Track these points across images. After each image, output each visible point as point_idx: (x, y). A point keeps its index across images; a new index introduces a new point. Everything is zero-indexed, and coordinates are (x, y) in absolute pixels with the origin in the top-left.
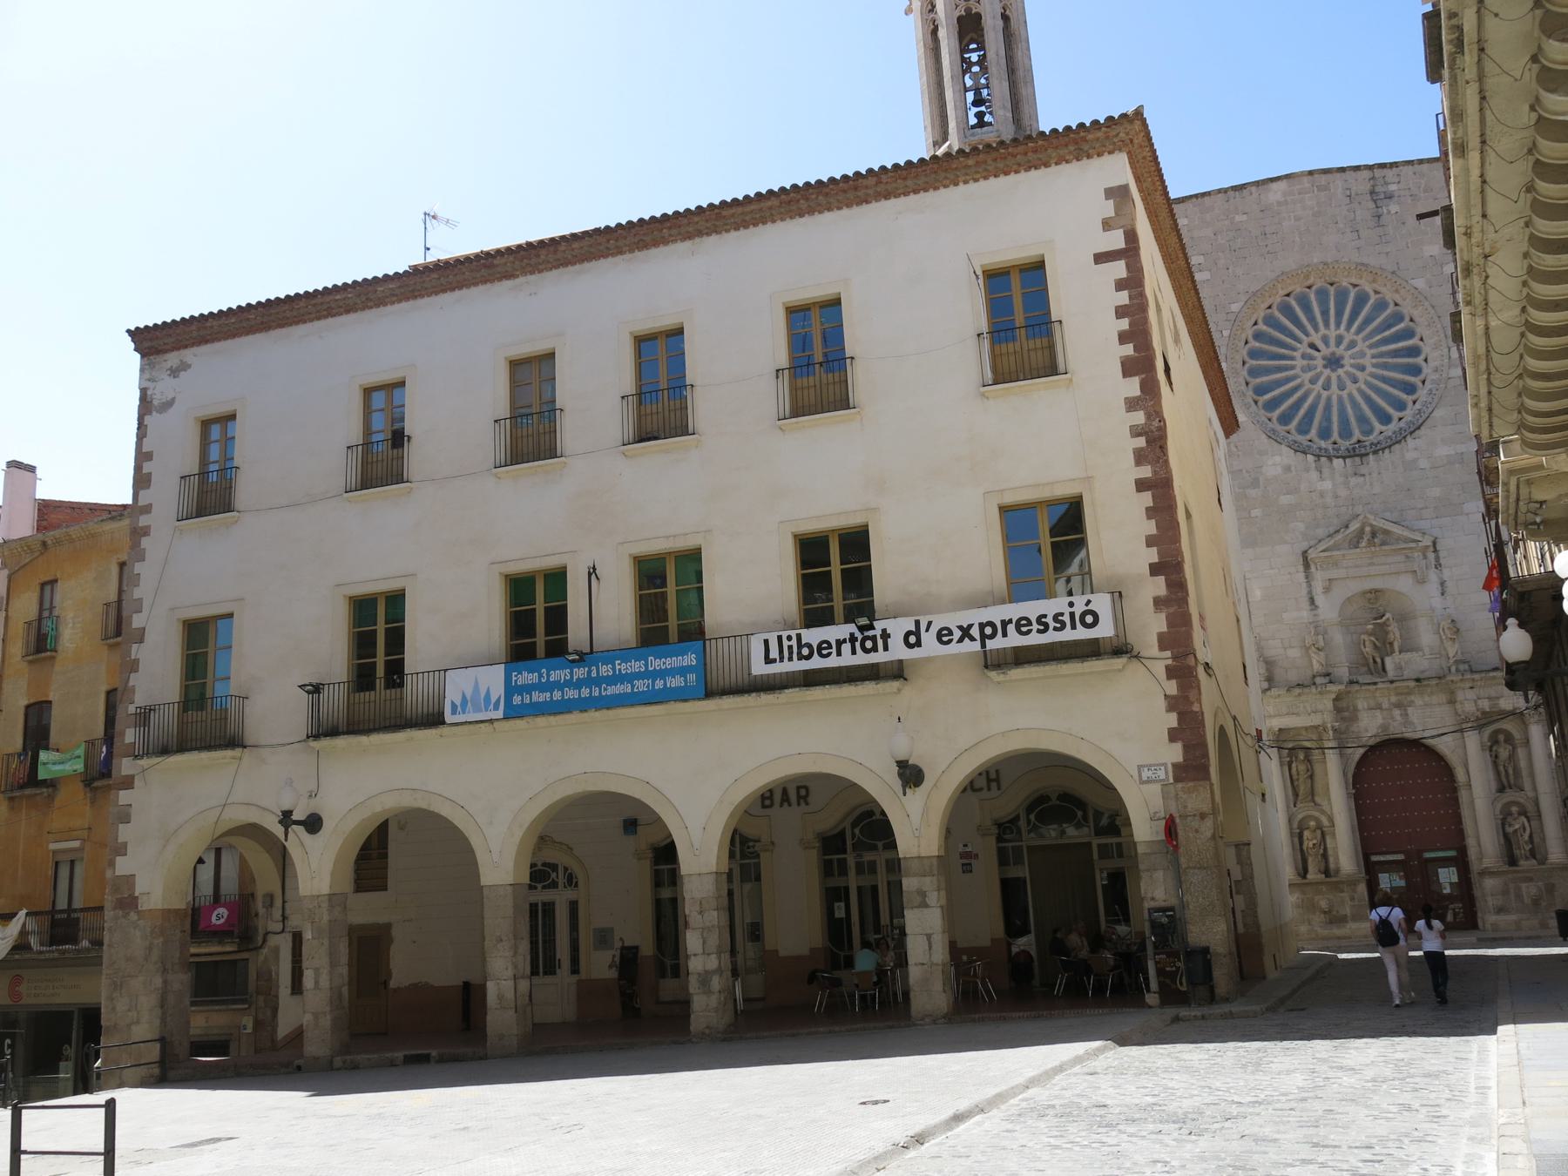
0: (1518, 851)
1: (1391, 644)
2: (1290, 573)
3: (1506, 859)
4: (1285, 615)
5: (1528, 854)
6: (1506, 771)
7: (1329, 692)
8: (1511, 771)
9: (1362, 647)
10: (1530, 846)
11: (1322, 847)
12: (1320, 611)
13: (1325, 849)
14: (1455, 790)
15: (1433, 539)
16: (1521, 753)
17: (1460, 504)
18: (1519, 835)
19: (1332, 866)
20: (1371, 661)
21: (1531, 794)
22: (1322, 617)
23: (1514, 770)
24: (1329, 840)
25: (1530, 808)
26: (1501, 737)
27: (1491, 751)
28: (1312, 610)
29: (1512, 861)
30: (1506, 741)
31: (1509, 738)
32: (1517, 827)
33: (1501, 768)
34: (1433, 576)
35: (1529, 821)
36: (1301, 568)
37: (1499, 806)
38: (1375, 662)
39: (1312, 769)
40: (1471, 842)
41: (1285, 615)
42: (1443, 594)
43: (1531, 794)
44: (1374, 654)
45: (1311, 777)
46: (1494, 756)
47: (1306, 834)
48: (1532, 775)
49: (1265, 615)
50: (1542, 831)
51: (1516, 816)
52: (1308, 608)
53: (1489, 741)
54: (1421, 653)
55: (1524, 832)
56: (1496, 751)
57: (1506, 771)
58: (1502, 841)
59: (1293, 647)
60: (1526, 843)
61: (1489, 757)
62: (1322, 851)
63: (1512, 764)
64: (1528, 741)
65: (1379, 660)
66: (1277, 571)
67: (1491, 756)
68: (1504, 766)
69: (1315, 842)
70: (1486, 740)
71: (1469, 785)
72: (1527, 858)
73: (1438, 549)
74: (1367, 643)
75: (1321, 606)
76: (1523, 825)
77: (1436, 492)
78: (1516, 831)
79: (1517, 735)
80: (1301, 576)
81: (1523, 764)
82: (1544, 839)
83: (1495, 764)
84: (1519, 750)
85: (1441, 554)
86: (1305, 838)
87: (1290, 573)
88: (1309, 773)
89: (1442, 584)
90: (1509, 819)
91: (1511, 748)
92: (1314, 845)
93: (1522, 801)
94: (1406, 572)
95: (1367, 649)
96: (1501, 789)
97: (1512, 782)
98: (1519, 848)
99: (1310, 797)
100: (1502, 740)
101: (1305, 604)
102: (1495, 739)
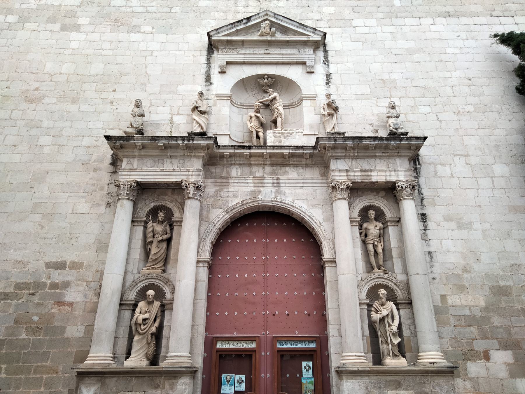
0: (385, 346)
1: (275, 122)
2: (193, 55)
3: (371, 355)
4: (179, 87)
5: (397, 352)
6: (375, 251)
7: (198, 147)
8: (380, 250)
9: (248, 123)
11: (157, 324)
12: (213, 87)
13: (160, 328)
14: (322, 269)
15: (322, 34)
16: (392, 231)
17: (350, 20)
18: (387, 325)
19: (163, 350)
20: (255, 135)
21: (401, 277)
22: (214, 92)
23: (384, 250)
24: (167, 313)
25: (400, 294)
26: (372, 214)
27: (360, 229)
28: (206, 86)
29: (378, 359)
30: (376, 219)
31: (380, 216)
32: (384, 312)
33: (371, 247)
34: (320, 69)
35: (398, 309)
36: (205, 53)
37: (366, 289)
38: (258, 137)
39: (172, 233)
40: (332, 330)
41: (179, 87)
42: (327, 84)
43: (401, 277)
44: (258, 130)
45: (169, 241)
46: (363, 234)
47: (142, 304)
48: (403, 256)
49: (162, 85)
50: (414, 323)
51: (384, 300)
52: (204, 83)
53: (359, 215)
54: (300, 130)
55: (393, 322)
56: (366, 229)
57: (375, 251)
58: (367, 333)
59: (181, 114)
60: (394, 334)
61: (358, 234)
62: (154, 329)
63: (382, 243)
64: (400, 218)
65: (261, 134)
66: (182, 53)
67: (361, 234)
68: (373, 244)
69: (147, 316)
70: (357, 216)
71: (334, 262)
72: (395, 356)
73: (327, 49)
74: (253, 119)
75: (215, 84)
76: (392, 312)
77: (332, 10)
78: (382, 320)
79: (389, 214)
80: (203, 59)
81: (394, 244)
82: (415, 333)
83: (364, 242)
84: (390, 228)
85: (330, 53)
86: (138, 310)
87: (193, 55)
88: (165, 237)
89: (328, 76)
90: (376, 304)
91: (381, 225)
92: (144, 320)
93: (391, 284)
94: (297, 63)
95: (252, 124)
96: (370, 268)
97: (381, 262)
98: (387, 342)
99: (161, 264)
100: (373, 216)
101: (202, 79)
102: (364, 213)
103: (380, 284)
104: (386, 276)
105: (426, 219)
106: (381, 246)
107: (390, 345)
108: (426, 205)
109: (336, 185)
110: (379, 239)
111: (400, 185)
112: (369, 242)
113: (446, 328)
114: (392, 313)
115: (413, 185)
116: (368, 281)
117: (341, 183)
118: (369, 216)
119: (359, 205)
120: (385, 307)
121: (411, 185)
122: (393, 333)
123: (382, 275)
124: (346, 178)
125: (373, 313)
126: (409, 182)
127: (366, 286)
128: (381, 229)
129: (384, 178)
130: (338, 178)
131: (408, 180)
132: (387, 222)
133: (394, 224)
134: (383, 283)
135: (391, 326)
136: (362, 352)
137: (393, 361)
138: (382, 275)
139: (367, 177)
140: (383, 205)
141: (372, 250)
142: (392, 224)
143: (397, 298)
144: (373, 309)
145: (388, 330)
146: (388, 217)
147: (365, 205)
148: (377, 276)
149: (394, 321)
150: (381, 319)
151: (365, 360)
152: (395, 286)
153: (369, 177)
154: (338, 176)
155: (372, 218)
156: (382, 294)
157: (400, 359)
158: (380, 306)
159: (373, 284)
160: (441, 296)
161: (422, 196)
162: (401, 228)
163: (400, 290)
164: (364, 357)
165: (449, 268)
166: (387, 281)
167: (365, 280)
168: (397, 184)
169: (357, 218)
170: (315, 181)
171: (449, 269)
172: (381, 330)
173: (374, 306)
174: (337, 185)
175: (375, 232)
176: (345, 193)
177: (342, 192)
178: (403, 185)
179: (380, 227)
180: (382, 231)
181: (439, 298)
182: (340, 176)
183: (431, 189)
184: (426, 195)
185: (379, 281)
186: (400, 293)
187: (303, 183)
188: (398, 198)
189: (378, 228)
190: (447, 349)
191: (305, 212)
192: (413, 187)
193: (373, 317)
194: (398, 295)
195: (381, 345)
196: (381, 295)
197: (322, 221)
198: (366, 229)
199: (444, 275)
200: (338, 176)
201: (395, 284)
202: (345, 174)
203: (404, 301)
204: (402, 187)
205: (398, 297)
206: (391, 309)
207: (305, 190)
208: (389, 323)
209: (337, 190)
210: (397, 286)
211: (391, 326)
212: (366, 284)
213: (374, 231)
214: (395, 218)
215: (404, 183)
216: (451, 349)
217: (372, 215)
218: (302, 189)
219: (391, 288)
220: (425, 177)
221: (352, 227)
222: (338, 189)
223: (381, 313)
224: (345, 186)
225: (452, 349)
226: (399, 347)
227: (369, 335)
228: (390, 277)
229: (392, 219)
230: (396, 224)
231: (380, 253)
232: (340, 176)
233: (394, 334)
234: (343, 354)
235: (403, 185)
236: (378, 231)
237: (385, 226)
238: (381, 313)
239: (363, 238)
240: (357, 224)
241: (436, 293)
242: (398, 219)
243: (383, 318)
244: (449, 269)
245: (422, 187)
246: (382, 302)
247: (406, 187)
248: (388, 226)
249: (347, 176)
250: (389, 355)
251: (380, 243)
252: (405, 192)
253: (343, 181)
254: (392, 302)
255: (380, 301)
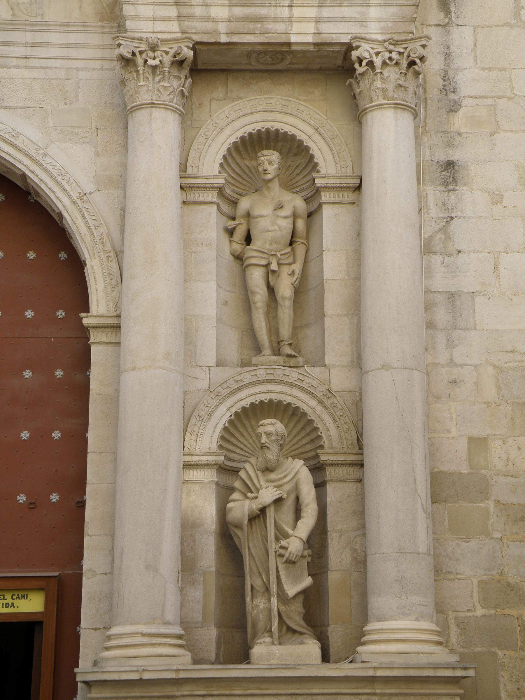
6: (271, 290)
10: (308, 581)
51: (272, 455)
56: (248, 215)
57: (271, 290)
63: (297, 267)
67: (231, 232)
76: (296, 488)
84: (327, 212)
97: (285, 332)
100: (272, 170)
103: (271, 401)
104: (293, 375)
105: (455, 181)
106: (293, 273)
107: (274, 601)
108: (463, 130)
109: (134, 54)
110: (289, 249)
111: (366, 55)
112: (253, 261)
113: (474, 544)
114: (297, 499)
115: (412, 55)
116: (228, 391)
117: (153, 48)
118: (261, 169)
119: (227, 131)
120: (273, 476)
121: (405, 55)
122: (288, 558)
123: (280, 372)
124: (174, 26)
125: (235, 496)
126: (397, 43)
127: (223, 408)
128: (299, 217)
129: (311, 28)
130: (148, 26)
131: (396, 37)
132: (318, 191)
133: (341, 199)
134: (281, 397)
135: (286, 536)
136: (168, 623)
137: (277, 649)
138: (279, 372)
139: (251, 26)
140: (310, 131)
141: (258, 290)
142: (337, 199)
143: (321, 447)
144: (237, 484)
145: (274, 550)
146: (323, 172)
147: (249, 129)
148: (262, 373)
149: (299, 523)
150: (258, 516)
151: (180, 646)
152: (319, 409)
153: (259, 25)
154: (147, 19)
155: (269, 177)
156: (268, 434)
157: (302, 643)
158: (259, 473)
159: (246, 403)
160: (471, 440)
161: (453, 97)
162: (361, 211)
163: (335, 421)
164: (180, 637)
165: (509, 348)
166: (296, 392)
167: (220, 389)
168: (354, 54)
169: (214, 177)
170: (73, 38)
171: (512, 352)
172: (253, 551)
173: (242, 474)
174: (141, 52)
175: (276, 228)
176: (166, 84)
177: (157, 79)
178: (377, 54)
179: (295, 209)
180: (301, 224)
181: (462, 446)
182: (154, 19)
183: (490, 69)
184: (468, 94)
185: (268, 392)
186: (333, 430)
187: (33, 45)
188: (363, 103)
189: (287, 211)
190: (469, 611)
191: (33, 152)
192: (412, 63)
193: (231, 509)
194: (325, 439)
195: (248, 600)
196: (264, 439)
197: (89, 187)
198: (248, 215)
199: (491, 370)
200: (147, 19)
201: (320, 402)
202: (173, 12)
203: (341, 458)
204: (371, 64)
205: (326, 445)
206: (292, 484)
207: (35, 73)
208: (277, 527)
209: (137, 72)
210: (325, 407)
211: (286, 536)
212: (221, 402)
213: (273, 223)
214: (347, 177)
215: (379, 49)
216: (480, 612)
217: (267, 166)
218: (26, 67)
219: (304, 414)
220: (475, 28)
221: (185, 207)
222: (141, 68)
223: (256, 498)
224: (167, 59)
225: (485, 612)
226: (306, 604)
227: (213, 569)
228: (307, 380)
229: (338, 181)
230: (348, 196)
231: (284, 298)
232: (154, 19)
233: (290, 562)
234: (115, 630)
235: (377, 54)
236: (286, 225)
237: (315, 205)
238: (256, 498)
239: (237, 247)
240: (215, 199)
241: (454, 430)
242: (357, 181)
243: (263, 510)
244: (512, 352)
245: (457, 62)
246: (266, 461)
247: (384, 63)
248: (320, 206)
249: (180, 17)
250: (270, 631)
251: (294, 262)
252: (378, 83)
253: (163, 40)
254: (302, 462)
255: (260, 459)
